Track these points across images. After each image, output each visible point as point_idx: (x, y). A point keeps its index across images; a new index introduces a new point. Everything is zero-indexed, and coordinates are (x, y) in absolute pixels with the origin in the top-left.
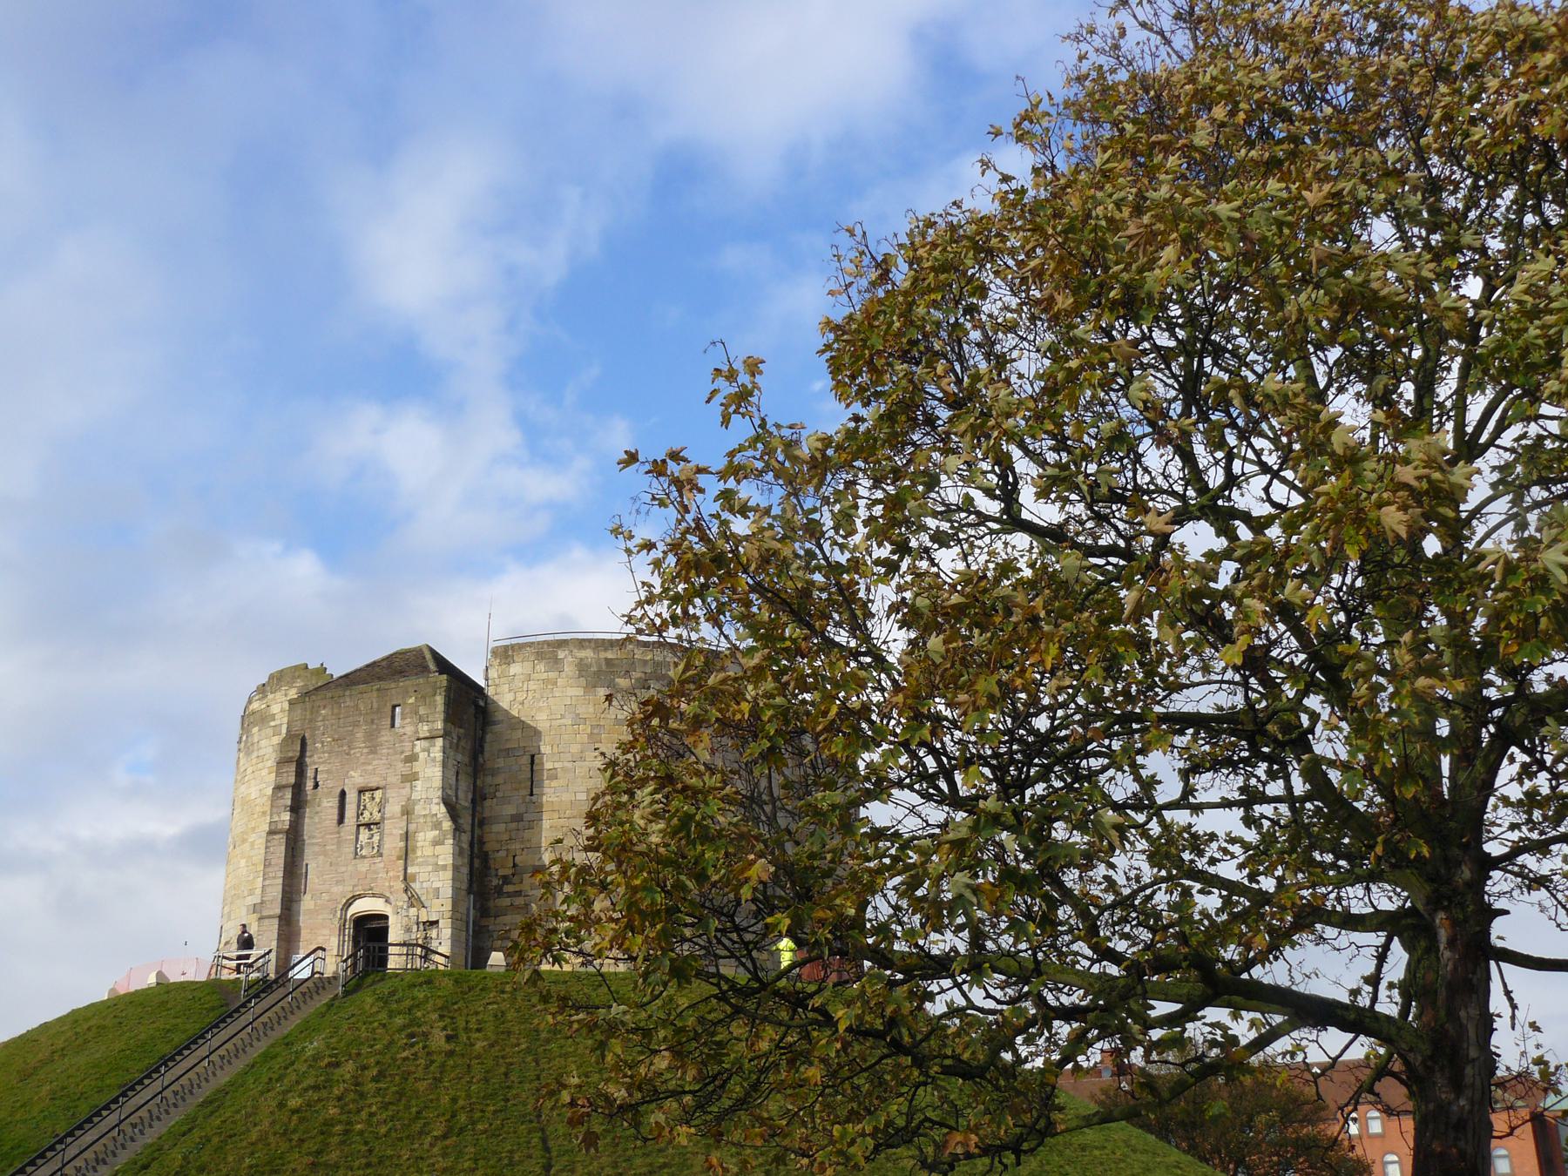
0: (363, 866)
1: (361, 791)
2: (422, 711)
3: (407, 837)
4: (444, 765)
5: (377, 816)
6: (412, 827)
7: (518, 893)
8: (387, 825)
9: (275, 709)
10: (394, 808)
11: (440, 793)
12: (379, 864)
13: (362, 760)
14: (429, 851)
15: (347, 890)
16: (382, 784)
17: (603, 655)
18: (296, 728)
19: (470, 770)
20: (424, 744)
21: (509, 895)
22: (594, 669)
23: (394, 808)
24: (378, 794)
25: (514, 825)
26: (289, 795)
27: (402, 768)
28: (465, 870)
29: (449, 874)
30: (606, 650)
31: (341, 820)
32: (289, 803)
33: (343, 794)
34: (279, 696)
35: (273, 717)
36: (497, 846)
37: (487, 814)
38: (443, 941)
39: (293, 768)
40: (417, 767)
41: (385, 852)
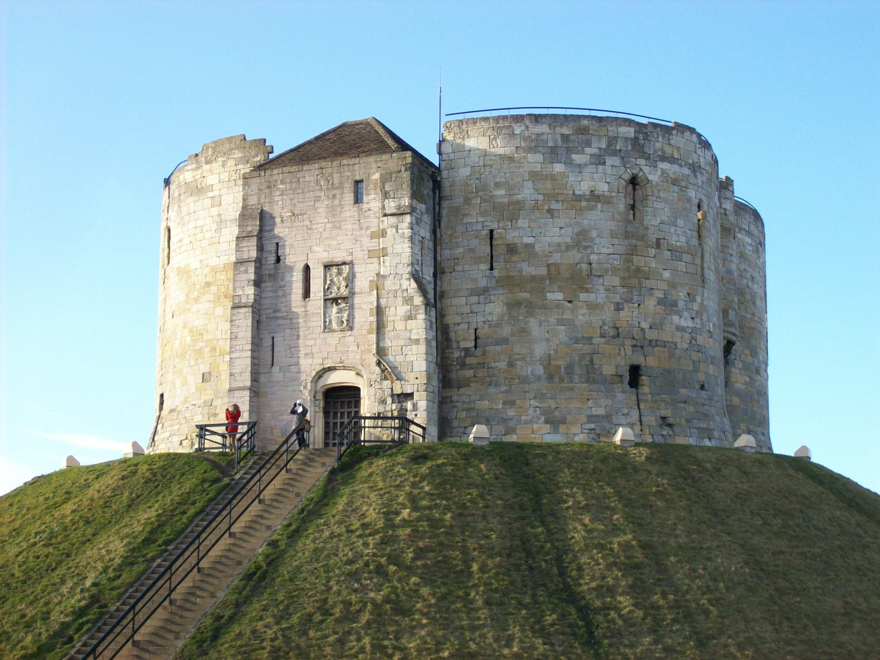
0: (333, 339)
1: (327, 267)
4: (411, 239)
5: (344, 292)
6: (383, 302)
7: (482, 365)
8: (357, 300)
10: (362, 283)
11: (409, 269)
12: (349, 338)
13: (325, 235)
14: (400, 326)
16: (348, 259)
17: (558, 129)
18: (253, 201)
19: (431, 245)
20: (393, 220)
21: (471, 367)
22: (550, 144)
24: (346, 269)
25: (474, 299)
26: (251, 269)
27: (370, 244)
28: (434, 344)
29: (422, 348)
30: (562, 125)
32: (252, 277)
33: (307, 268)
34: (216, 166)
35: (211, 188)
36: (458, 319)
37: (446, 286)
38: (420, 411)
39: (254, 242)
41: (356, 326)
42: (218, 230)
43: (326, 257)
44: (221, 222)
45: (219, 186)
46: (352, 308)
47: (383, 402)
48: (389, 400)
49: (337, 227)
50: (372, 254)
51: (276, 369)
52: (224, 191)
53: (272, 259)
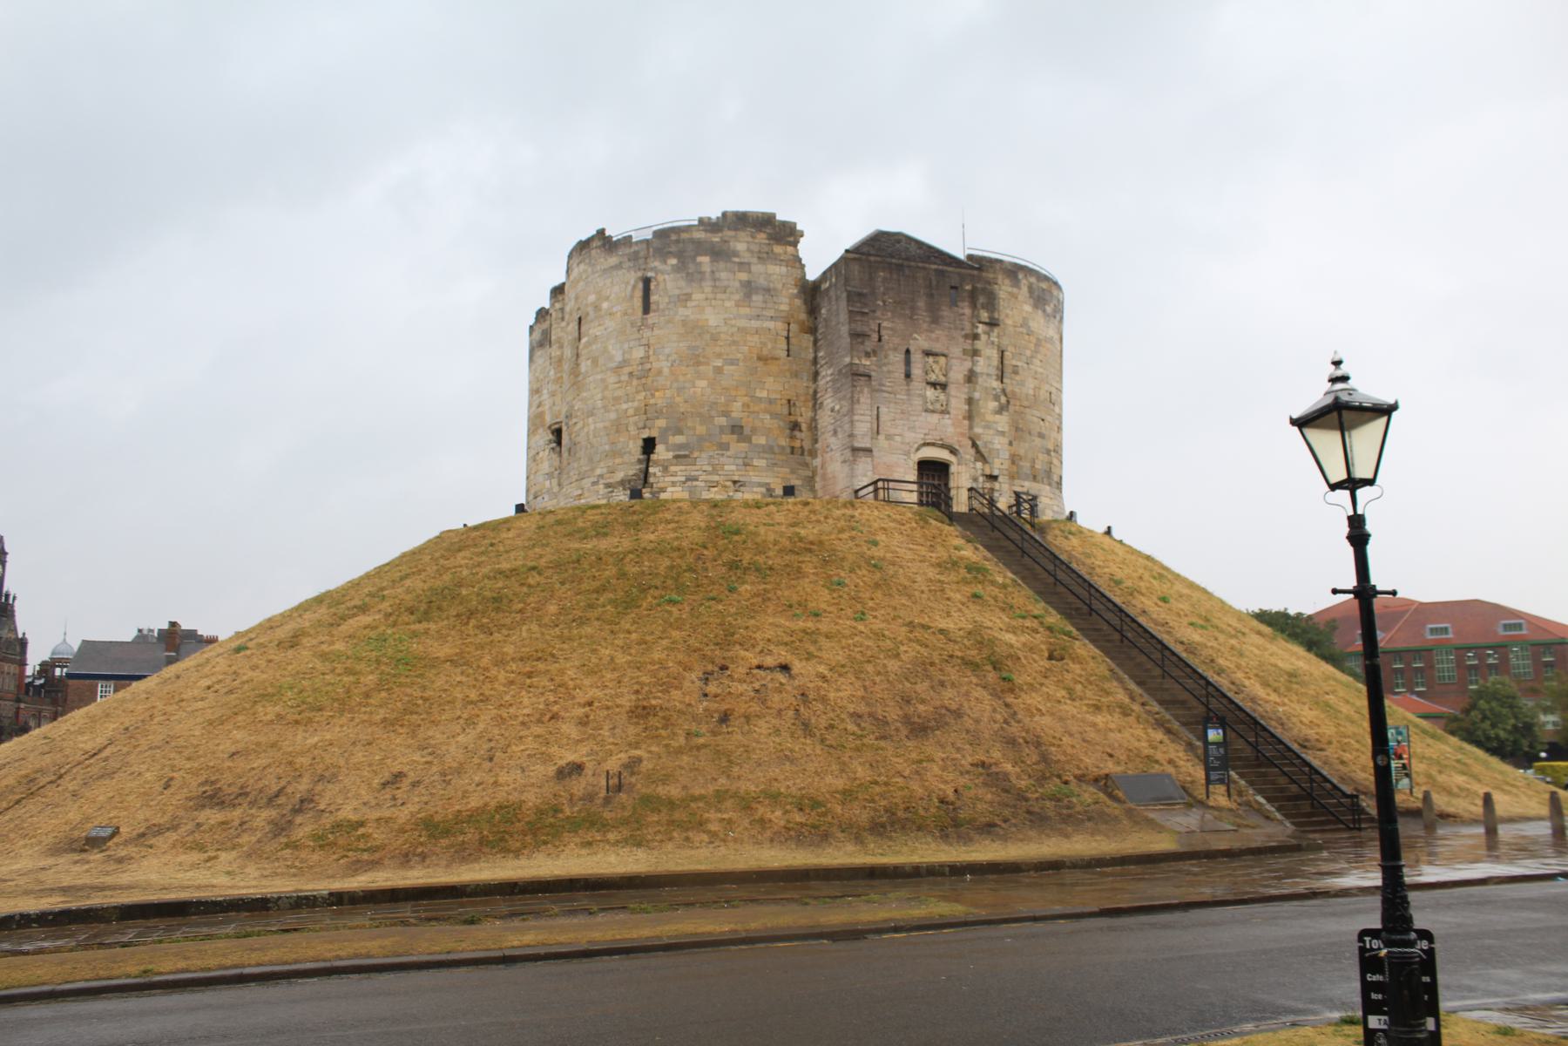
1: (928, 354)
2: (982, 300)
3: (970, 401)
5: (942, 379)
6: (977, 395)
8: (952, 389)
9: (741, 247)
12: (947, 421)
15: (919, 438)
23: (958, 373)
24: (942, 360)
31: (908, 376)
33: (908, 352)
34: (744, 235)
35: (736, 254)
40: (979, 345)
42: (748, 296)
43: (926, 345)
44: (749, 288)
45: (747, 255)
46: (948, 396)
47: (975, 480)
48: (981, 479)
49: (935, 320)
50: (965, 352)
51: (881, 437)
52: (755, 260)
53: (875, 336)
